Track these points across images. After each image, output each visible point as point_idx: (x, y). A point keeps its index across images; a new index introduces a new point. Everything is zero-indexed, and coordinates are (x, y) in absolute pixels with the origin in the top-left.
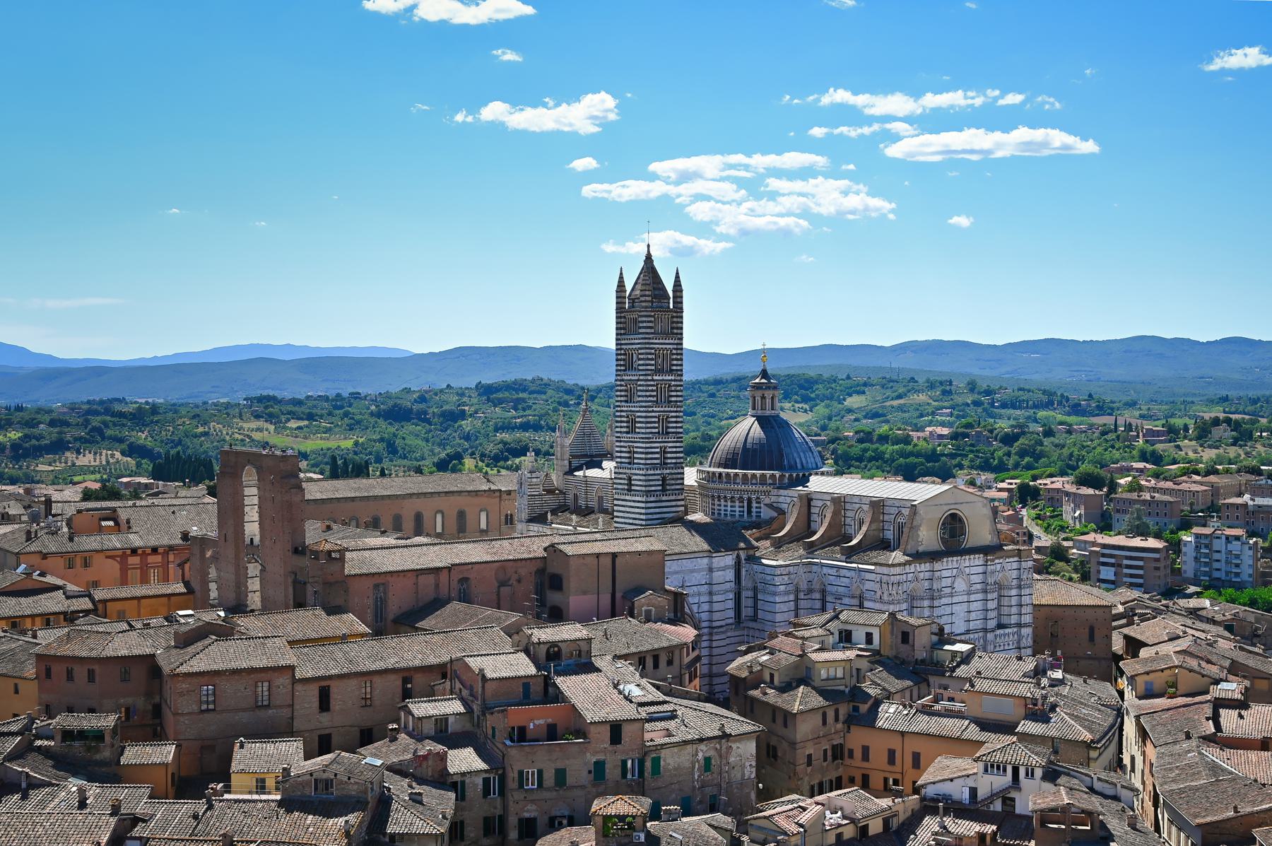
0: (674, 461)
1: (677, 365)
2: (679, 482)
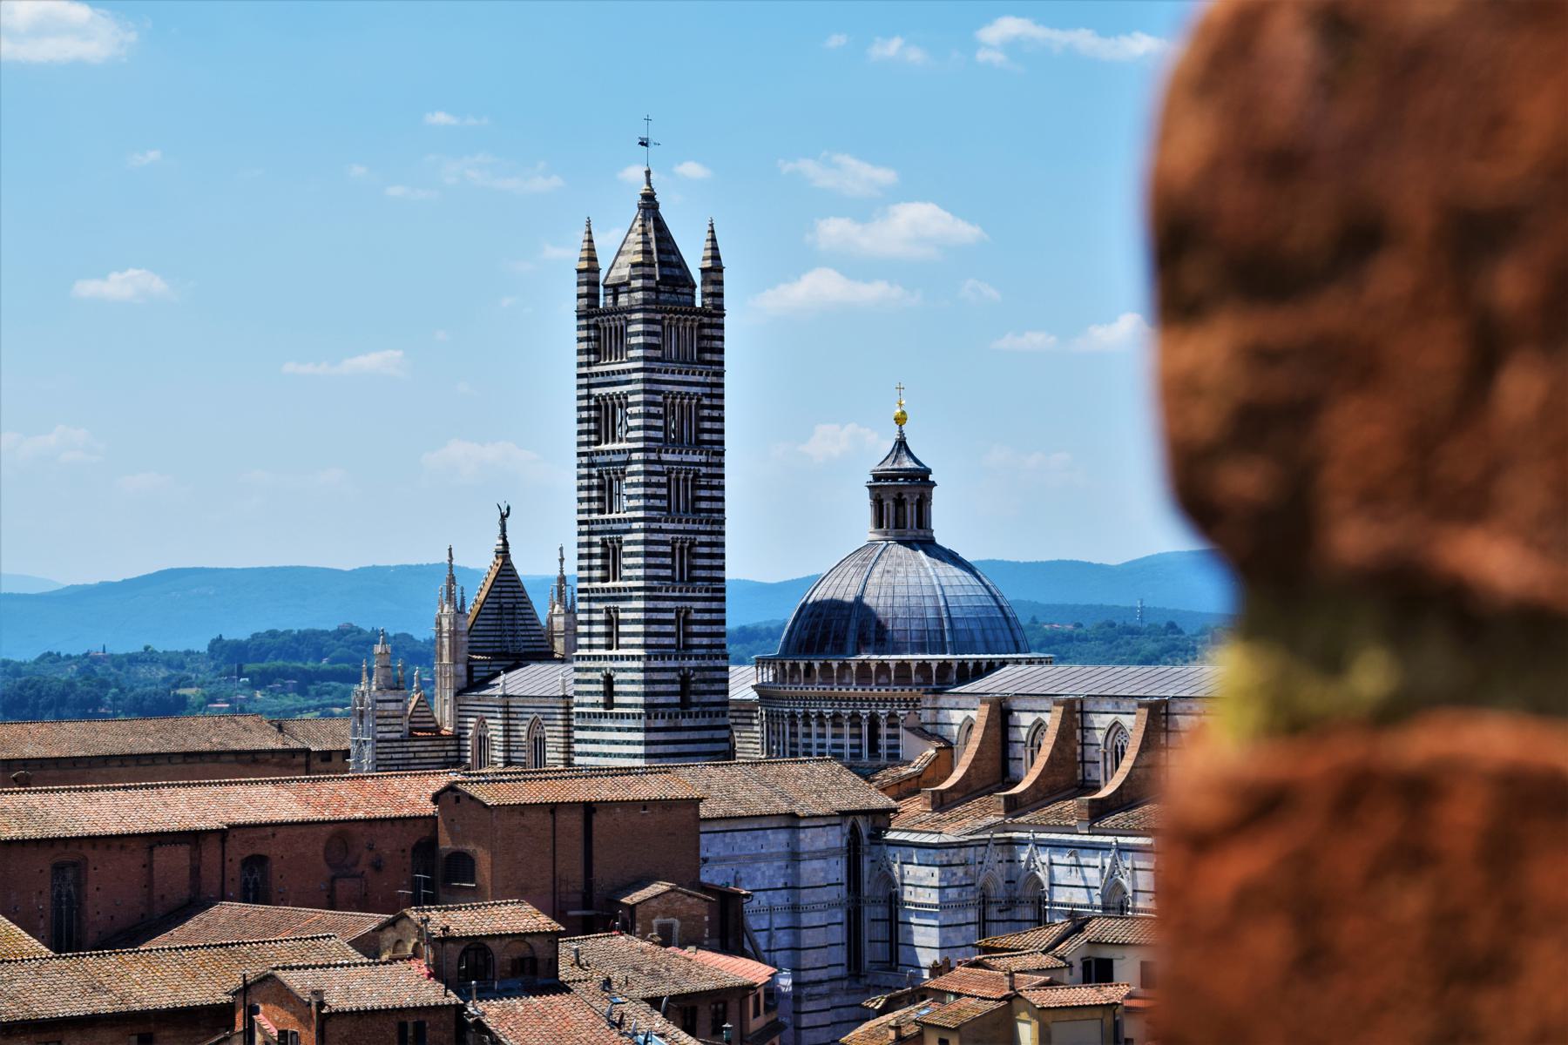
0: (705, 641)
1: (711, 431)
2: (717, 687)
